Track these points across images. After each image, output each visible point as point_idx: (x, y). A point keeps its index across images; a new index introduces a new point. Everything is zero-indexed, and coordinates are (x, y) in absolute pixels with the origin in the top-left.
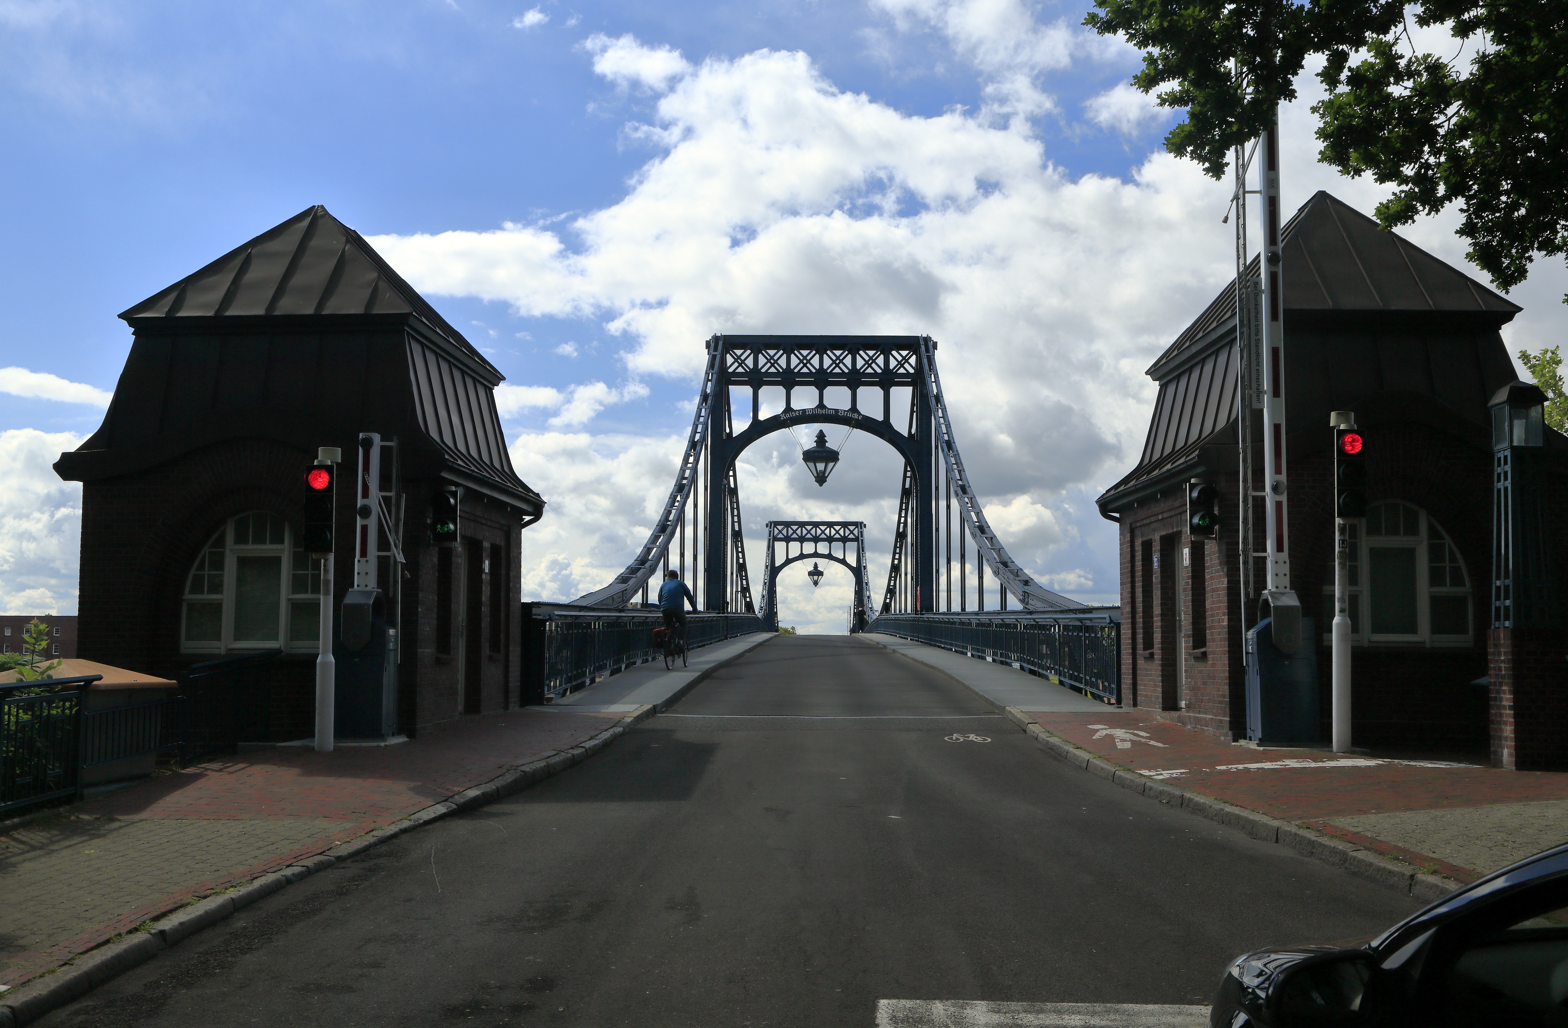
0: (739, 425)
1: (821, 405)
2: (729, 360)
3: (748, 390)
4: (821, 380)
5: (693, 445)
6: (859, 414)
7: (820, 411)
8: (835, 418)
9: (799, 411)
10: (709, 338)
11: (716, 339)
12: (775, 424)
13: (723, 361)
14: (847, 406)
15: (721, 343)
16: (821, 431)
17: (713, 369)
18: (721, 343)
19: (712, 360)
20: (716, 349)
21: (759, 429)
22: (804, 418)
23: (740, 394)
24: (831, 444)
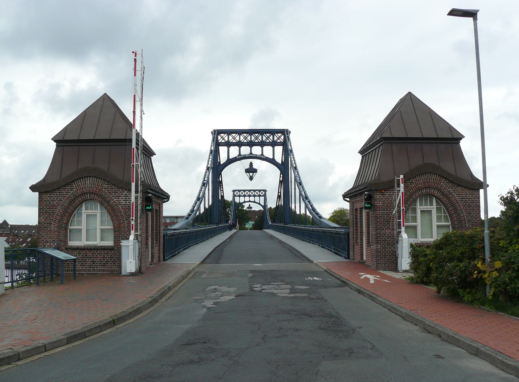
0: (223, 159)
1: (251, 153)
2: (219, 137)
3: (226, 148)
4: (251, 144)
5: (208, 168)
6: (264, 156)
7: (251, 155)
8: (256, 157)
9: (243, 155)
10: (212, 130)
11: (215, 131)
12: (235, 160)
13: (217, 138)
14: (260, 153)
15: (216, 132)
16: (251, 162)
17: (214, 142)
18: (216, 132)
19: (214, 138)
20: (214, 135)
21: (230, 161)
22: (245, 157)
23: (223, 150)
24: (255, 167)
